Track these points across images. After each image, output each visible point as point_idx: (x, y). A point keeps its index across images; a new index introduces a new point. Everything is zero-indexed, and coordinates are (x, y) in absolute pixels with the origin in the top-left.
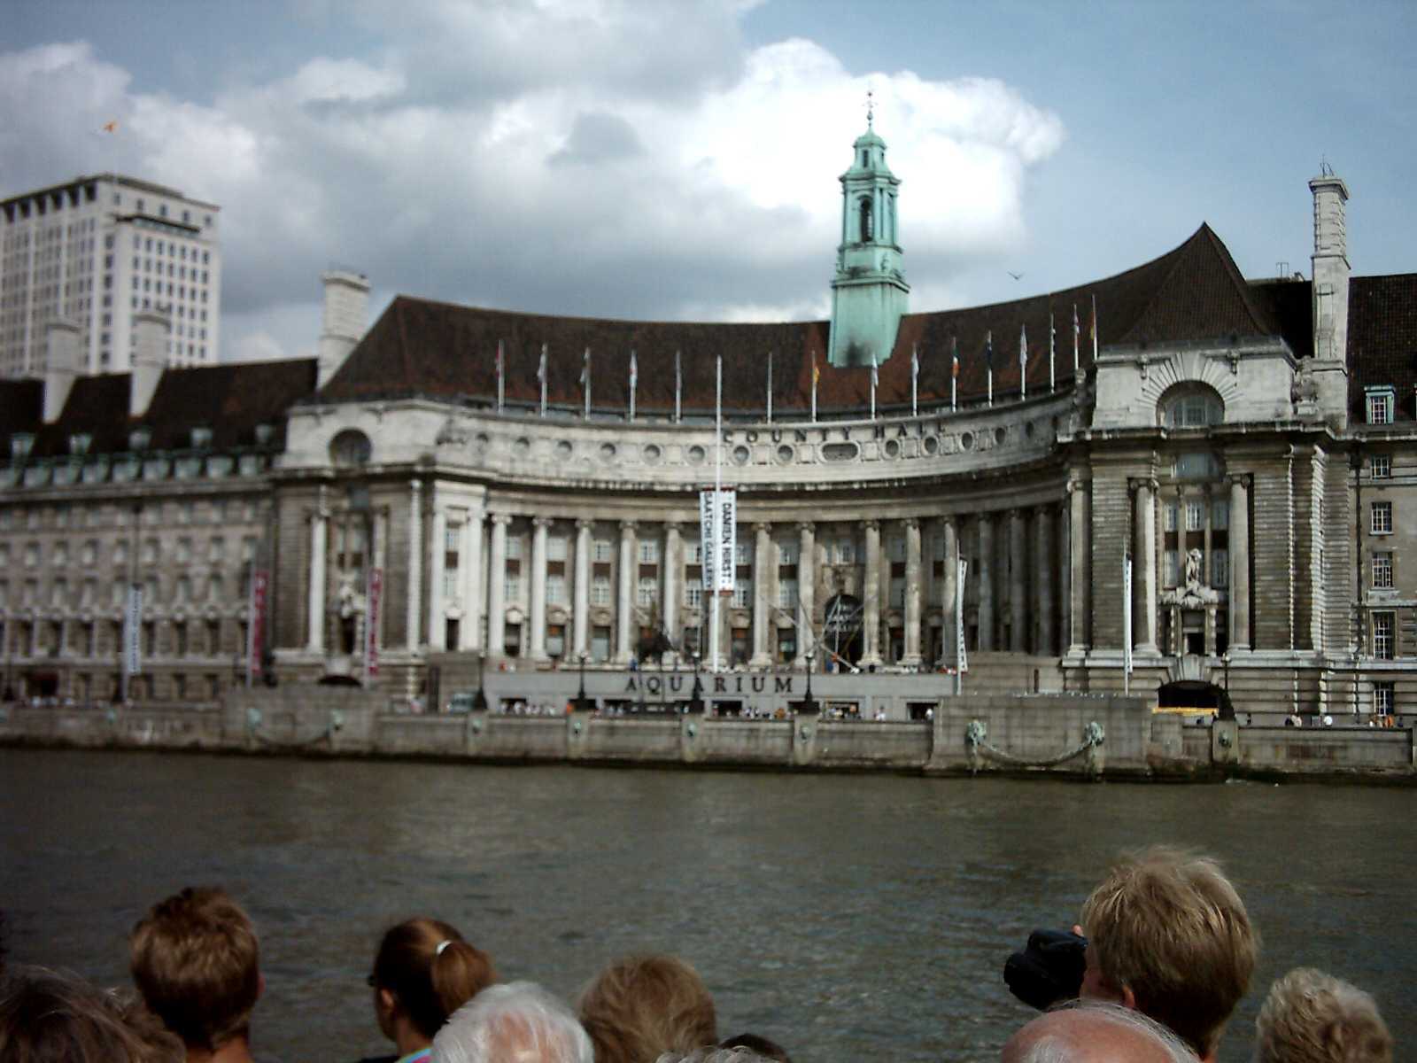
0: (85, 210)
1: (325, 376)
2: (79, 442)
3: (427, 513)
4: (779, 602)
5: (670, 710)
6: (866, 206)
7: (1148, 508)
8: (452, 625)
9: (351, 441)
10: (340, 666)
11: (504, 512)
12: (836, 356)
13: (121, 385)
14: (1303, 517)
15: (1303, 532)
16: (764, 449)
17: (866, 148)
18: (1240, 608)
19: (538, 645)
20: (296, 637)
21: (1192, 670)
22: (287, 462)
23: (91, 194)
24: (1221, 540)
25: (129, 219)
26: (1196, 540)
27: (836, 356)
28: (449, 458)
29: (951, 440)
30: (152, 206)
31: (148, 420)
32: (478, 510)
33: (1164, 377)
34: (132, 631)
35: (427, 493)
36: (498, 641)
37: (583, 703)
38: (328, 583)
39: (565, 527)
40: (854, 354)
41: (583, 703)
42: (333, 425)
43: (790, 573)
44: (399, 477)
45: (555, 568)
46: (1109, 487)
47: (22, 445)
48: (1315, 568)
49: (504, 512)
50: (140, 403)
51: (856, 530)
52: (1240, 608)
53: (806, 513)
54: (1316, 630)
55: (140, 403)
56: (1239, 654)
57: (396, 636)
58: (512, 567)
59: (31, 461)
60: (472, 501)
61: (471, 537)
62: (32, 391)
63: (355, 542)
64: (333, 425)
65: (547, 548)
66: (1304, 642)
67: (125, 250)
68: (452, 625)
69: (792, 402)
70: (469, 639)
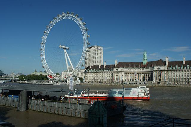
0: (94, 48)
1: (115, 66)
4: (140, 77)
7: (157, 74)
9: (117, 70)
12: (143, 64)
13: (104, 66)
16: (139, 69)
19: (127, 80)
20: (114, 80)
22: (113, 71)
23: (94, 47)
26: (159, 75)
27: (143, 64)
28: (123, 71)
29: (149, 69)
31: (105, 68)
32: (124, 73)
37: (129, 83)
41: (129, 83)
43: (141, 76)
45: (128, 76)
46: (155, 73)
47: (98, 69)
48: (165, 76)
50: (105, 67)
51: (144, 74)
52: (161, 79)
53: (141, 73)
55: (105, 67)
56: (161, 81)
58: (126, 76)
59: (99, 70)
60: (124, 73)
62: (98, 66)
63: (117, 75)
65: (127, 75)
66: (164, 80)
67: (97, 51)
70: (123, 80)
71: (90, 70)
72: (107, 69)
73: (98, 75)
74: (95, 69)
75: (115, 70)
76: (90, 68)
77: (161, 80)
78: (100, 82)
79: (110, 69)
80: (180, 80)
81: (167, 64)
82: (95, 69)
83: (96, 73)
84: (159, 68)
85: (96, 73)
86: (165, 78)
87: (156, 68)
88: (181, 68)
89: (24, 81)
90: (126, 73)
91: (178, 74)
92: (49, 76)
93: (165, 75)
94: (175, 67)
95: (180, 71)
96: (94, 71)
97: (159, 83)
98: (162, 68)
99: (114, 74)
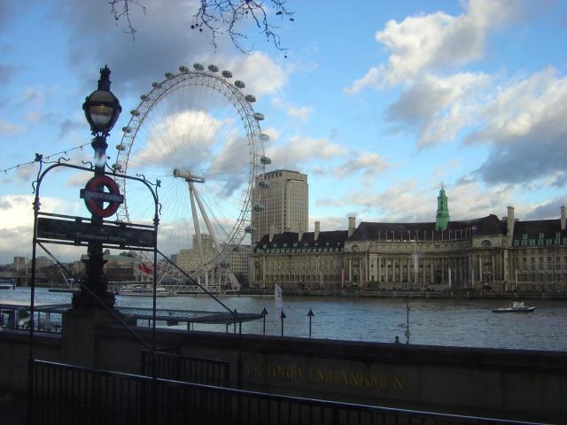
0: (279, 178)
2: (306, 245)
3: (368, 259)
5: (408, 291)
6: (442, 203)
8: (373, 277)
10: (355, 284)
11: (381, 257)
12: (437, 229)
14: (503, 260)
15: (503, 263)
17: (442, 192)
18: (494, 274)
21: (486, 284)
23: (281, 174)
24: (491, 264)
25: (289, 180)
30: (294, 176)
31: (318, 241)
33: (483, 239)
34: (321, 278)
35: (368, 256)
36: (380, 279)
38: (352, 271)
39: (392, 260)
40: (440, 228)
42: (352, 244)
44: (364, 253)
47: (295, 245)
49: (381, 257)
50: (316, 238)
54: (505, 278)
55: (316, 238)
57: (364, 278)
58: (382, 266)
60: (376, 256)
61: (376, 262)
64: (352, 244)
66: (503, 279)
68: (373, 277)
69: (429, 237)
70: (376, 279)
71: (270, 246)
72: (324, 246)
73: (296, 262)
74: (285, 245)
75: (348, 247)
76: (271, 240)
77: (494, 280)
78: (303, 285)
79: (334, 246)
80: (550, 281)
81: (511, 227)
82: (285, 245)
83: (290, 256)
84: (488, 243)
85: (290, 256)
86: (506, 273)
87: (477, 242)
88: (553, 242)
89: (65, 282)
90: (385, 257)
91: (545, 259)
92: (140, 268)
93: (506, 264)
94: (536, 237)
95: (551, 249)
96: (283, 251)
97: (489, 288)
98: (496, 241)
99: (345, 259)
